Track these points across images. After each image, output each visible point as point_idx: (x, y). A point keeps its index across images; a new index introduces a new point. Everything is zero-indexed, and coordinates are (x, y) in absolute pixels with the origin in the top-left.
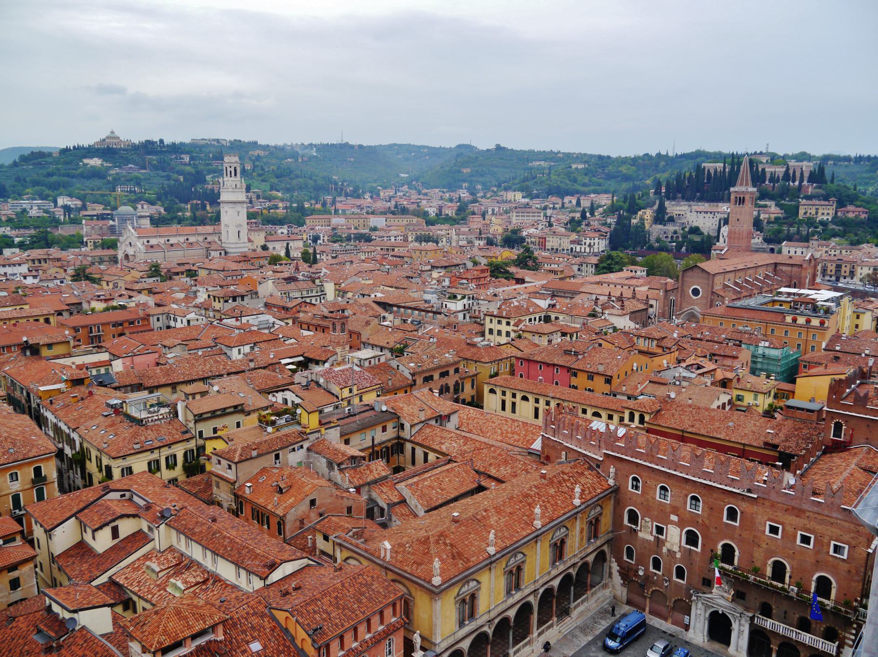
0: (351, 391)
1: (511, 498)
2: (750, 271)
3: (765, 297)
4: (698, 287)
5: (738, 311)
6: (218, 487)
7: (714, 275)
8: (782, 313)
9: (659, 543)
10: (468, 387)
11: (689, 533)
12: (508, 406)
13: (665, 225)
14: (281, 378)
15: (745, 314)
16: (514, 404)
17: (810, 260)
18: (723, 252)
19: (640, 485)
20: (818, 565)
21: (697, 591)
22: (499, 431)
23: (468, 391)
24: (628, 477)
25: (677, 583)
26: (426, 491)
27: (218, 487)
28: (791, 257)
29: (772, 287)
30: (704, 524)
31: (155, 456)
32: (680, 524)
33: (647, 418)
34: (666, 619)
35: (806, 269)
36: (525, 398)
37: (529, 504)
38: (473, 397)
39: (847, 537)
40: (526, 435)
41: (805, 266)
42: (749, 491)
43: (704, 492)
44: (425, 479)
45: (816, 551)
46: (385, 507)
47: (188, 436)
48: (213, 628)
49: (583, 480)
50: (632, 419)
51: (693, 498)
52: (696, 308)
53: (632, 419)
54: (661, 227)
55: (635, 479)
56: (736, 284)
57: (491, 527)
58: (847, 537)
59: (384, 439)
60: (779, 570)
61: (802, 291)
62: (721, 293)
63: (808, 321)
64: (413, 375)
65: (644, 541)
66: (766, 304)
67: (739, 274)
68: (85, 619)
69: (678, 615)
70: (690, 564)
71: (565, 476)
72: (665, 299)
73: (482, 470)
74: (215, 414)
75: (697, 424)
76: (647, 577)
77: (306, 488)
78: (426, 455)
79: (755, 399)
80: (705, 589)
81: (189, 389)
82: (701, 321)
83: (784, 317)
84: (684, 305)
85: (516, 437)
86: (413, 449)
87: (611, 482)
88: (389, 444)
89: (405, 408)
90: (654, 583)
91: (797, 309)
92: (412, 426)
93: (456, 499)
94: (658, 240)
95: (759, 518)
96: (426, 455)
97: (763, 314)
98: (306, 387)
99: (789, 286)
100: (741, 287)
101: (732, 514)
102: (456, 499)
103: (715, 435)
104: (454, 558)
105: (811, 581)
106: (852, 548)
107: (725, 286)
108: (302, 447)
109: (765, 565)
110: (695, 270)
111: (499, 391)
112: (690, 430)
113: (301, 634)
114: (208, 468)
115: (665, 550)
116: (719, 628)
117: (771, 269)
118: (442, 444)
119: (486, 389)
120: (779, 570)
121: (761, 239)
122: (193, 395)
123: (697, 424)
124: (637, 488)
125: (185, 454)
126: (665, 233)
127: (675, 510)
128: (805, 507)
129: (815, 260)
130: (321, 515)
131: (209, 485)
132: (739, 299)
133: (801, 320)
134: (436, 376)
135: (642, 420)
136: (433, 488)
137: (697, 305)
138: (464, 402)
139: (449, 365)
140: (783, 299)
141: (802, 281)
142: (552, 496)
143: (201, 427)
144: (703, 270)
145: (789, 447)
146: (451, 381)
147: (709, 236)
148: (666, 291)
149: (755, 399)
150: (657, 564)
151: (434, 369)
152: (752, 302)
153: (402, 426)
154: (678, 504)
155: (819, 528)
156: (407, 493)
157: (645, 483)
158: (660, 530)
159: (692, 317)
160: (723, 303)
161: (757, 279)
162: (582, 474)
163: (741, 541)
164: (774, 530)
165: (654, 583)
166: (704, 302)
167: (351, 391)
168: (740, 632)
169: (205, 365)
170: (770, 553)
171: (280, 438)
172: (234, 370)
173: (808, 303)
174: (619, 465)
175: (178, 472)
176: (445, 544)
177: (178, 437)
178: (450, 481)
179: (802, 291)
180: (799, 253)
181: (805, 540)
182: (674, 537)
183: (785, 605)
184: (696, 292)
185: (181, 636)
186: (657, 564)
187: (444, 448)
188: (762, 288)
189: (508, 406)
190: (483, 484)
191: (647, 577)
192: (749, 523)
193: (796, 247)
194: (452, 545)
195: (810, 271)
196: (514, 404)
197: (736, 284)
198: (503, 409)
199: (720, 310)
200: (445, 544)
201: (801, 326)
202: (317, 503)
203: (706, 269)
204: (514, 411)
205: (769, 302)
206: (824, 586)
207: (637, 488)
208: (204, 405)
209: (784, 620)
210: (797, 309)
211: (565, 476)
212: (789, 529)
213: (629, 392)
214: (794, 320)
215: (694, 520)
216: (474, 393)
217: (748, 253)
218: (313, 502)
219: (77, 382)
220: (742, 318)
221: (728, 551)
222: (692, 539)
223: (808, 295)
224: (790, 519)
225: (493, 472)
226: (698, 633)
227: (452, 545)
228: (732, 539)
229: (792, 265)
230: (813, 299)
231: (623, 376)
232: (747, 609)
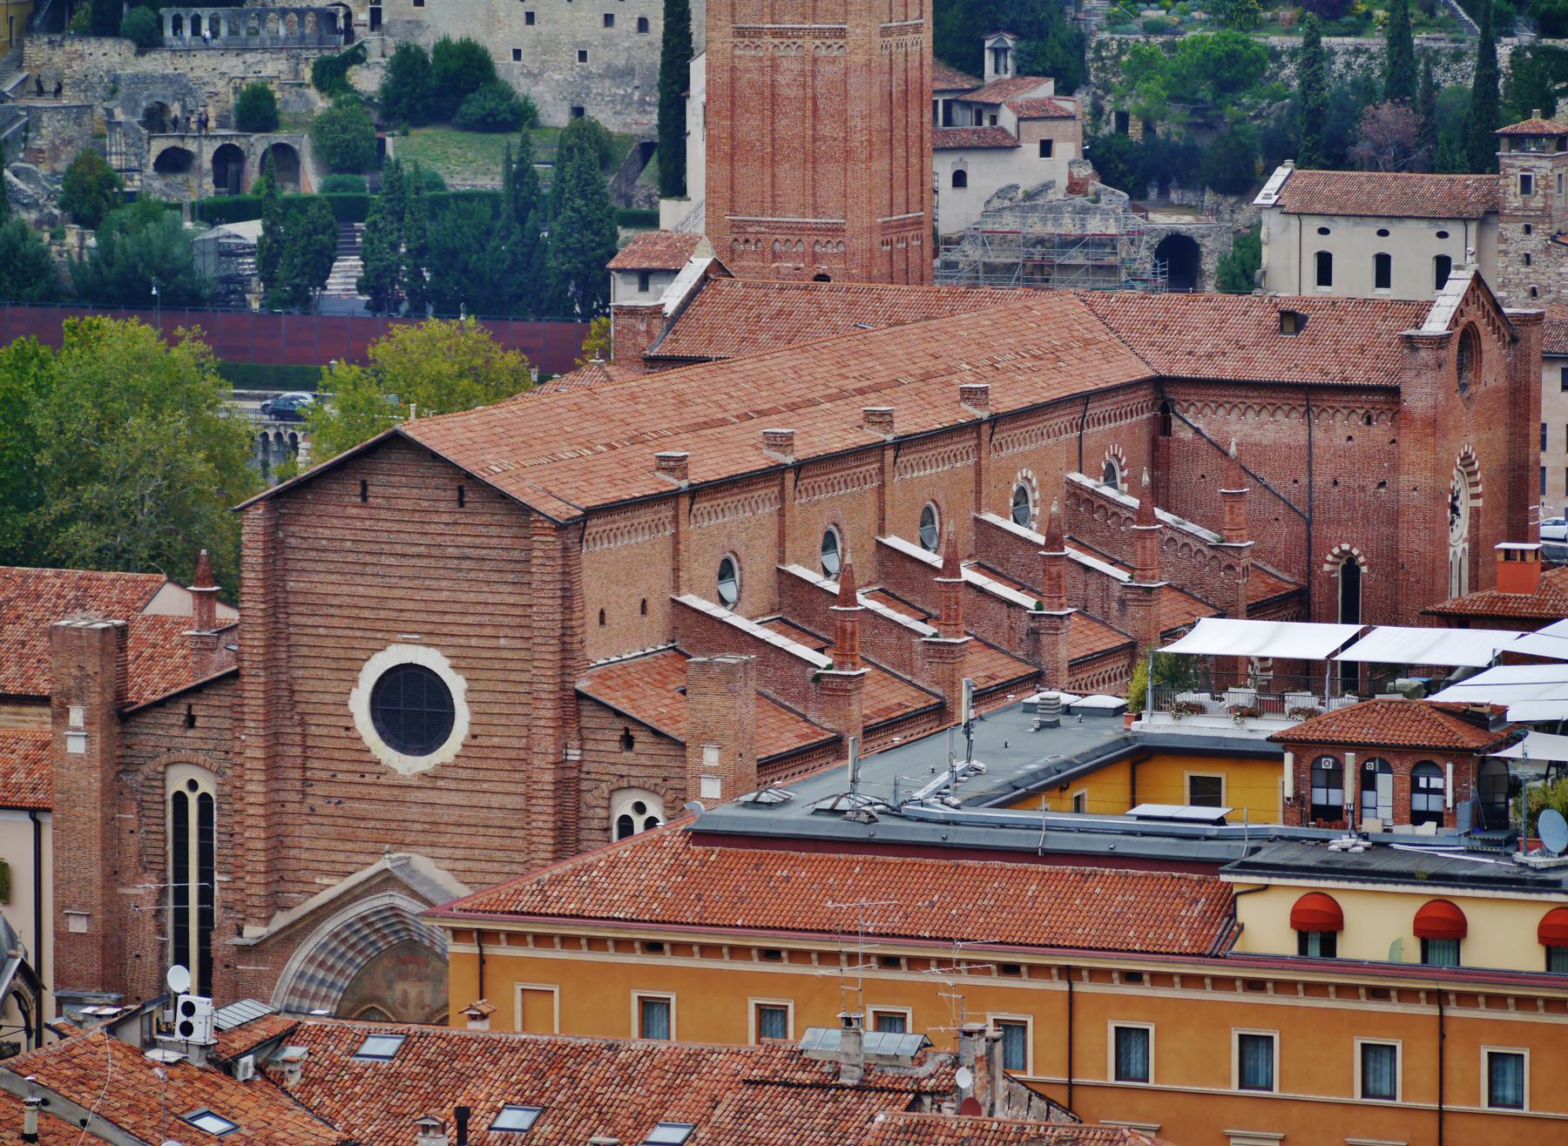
2: (926, 476)
3: (1053, 719)
4: (433, 659)
5: (799, 869)
7: (576, 527)
8: (1204, 872)
13: (148, 41)
15: (864, 899)
17: (1466, 339)
18: (671, 296)
28: (1292, 320)
29: (1135, 622)
35: (1434, 425)
41: (1420, 396)
52: (433, 872)
54: (108, 56)
56: (795, 603)
61: (1387, 644)
62: (651, 706)
63: (1442, 931)
66: (1061, 782)
67: (817, 507)
72: (114, 793)
82: (460, 990)
83: (1227, 905)
84: (308, 843)
91: (1331, 816)
94: (90, 195)
97: (1034, 882)
99: (1296, 605)
100: (836, 640)
107: (694, 634)
110: (395, 487)
117: (1120, 434)
121: (1067, 150)
126: (156, 119)
129: (1514, 331)
132: (834, 747)
133: (1378, 927)
137: (432, 834)
140: (1214, 724)
141: (1413, 541)
144: (467, 486)
147: (587, 144)
148: (124, 716)
152: (920, 779)
159: (388, 960)
160: (676, 804)
161: (993, 549)
166: (502, 797)
173: (1425, 759)
179: (1387, 644)
180: (1354, 278)
184: (412, 707)
188: (1039, 630)
193: (1385, 219)
195: (1475, 440)
197: (795, 603)
199: (625, 875)
201: (1379, 984)
203: (494, 467)
205: (1094, 768)
210: (1331, 816)
214: (1319, 928)
217: (905, 296)
220: (824, 944)
223: (1441, 676)
229: (1309, 396)
230: (1473, 716)
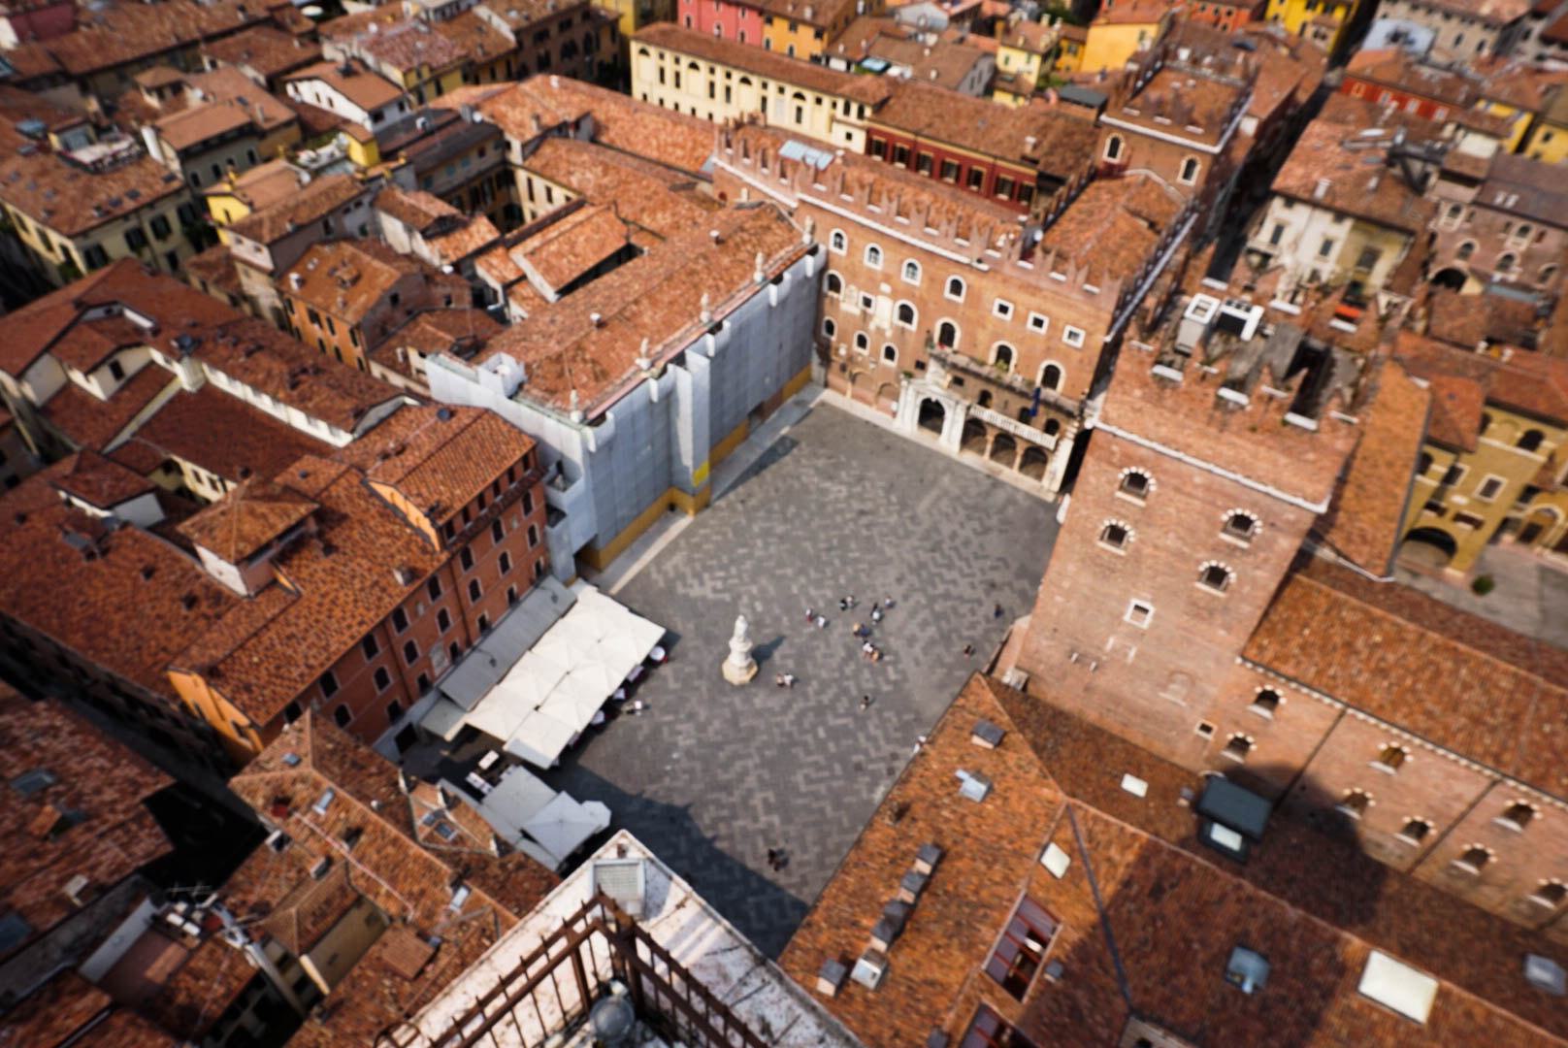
0: (419, 75)
1: (669, 278)
6: (248, 275)
9: (865, 317)
11: (904, 308)
16: (678, 75)
19: (845, 243)
20: (1048, 352)
21: (909, 375)
22: (654, 143)
24: (828, 231)
25: (886, 369)
26: (554, 261)
27: (248, 275)
30: (921, 298)
31: (132, 223)
32: (894, 295)
33: (868, 112)
34: (869, 403)
37: (695, 286)
38: (615, 57)
39: (1084, 323)
40: (694, 149)
42: (980, 261)
43: (924, 257)
44: (550, 241)
45: (1049, 338)
46: (498, 287)
47: (175, 185)
48: (301, 522)
49: (769, 238)
50: (847, 111)
51: (911, 265)
53: (847, 111)
55: (838, 235)
57: (644, 326)
58: (1084, 323)
59: (483, 167)
60: (1004, 354)
64: (517, 33)
65: (848, 315)
68: (125, 511)
69: (884, 401)
70: (902, 343)
71: (746, 236)
73: (631, 218)
74: (207, 146)
75: (937, 122)
76: (851, 358)
77: (382, 279)
78: (549, 191)
79: (1029, 62)
80: (917, 372)
85: (679, 152)
86: (530, 181)
87: (806, 238)
88: (493, 174)
89: (510, 114)
90: (858, 364)
92: (524, 146)
93: (596, 272)
95: (987, 295)
96: (549, 191)
98: (348, 72)
101: (956, 287)
102: (596, 272)
103: (958, 140)
104: (597, 379)
105: (1036, 369)
106: (1089, 334)
108: (359, 204)
109: (988, 349)
112: (926, 132)
113: (416, 515)
115: (872, 326)
116: (931, 414)
118: (570, 173)
119: (635, 47)
120: (1004, 354)
123: (937, 122)
124: (840, 246)
125: (180, 212)
127: (887, 278)
128: (1044, 284)
130: (409, 313)
134: (554, 30)
135: (861, 114)
136: (563, 256)
139: (571, 9)
142: (727, 270)
145: (1052, 164)
149: (1029, 62)
150: (862, 342)
151: (549, 20)
153: (508, 146)
154: (891, 271)
155: (1056, 310)
156: (526, 266)
157: (851, 241)
158: (867, 302)
162: (769, 228)
163: (965, 321)
164: (1003, 309)
165: (858, 364)
167: (419, 75)
168: (953, 422)
169: (162, 22)
170: (996, 336)
171: (326, 193)
172: (214, 29)
174: (818, 215)
176: (585, 361)
177: (160, 188)
178: (587, 240)
181: (1038, 323)
182: (885, 312)
183: (1007, 395)
185: (264, 540)
186: (862, 342)
187: (574, 180)
190: (633, 240)
191: (851, 358)
192: (975, 300)
194: (594, 362)
196: (678, 75)
198: (662, 80)
200: (585, 361)
202: (401, 298)
204: (678, 85)
206: (1051, 376)
207: (840, 246)
209: (1004, 410)
211: (746, 236)
212: (1020, 308)
213: (849, 54)
215: (909, 292)
216: (615, 49)
218: (395, 299)
221: (947, 334)
222: (906, 314)
224: (1023, 298)
225: (646, 221)
226: (905, 422)
227: (594, 362)
228: (954, 316)
231: (841, 24)
232: (965, 397)
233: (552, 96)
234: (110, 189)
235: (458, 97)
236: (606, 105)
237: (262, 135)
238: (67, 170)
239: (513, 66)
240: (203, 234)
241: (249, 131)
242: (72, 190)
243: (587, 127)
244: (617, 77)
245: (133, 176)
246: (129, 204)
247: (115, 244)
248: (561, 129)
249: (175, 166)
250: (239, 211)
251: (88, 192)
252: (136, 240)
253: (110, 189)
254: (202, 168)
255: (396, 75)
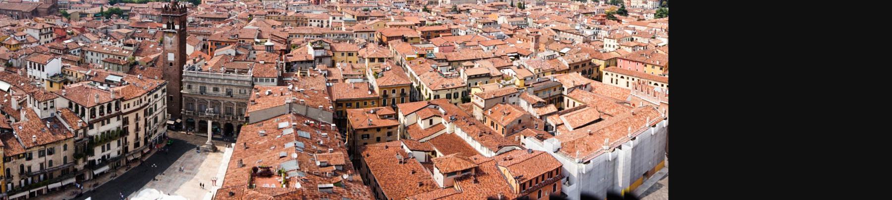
10: (595, 72)
12: (614, 81)
14: (506, 63)
23: (595, 74)
36: (622, 77)
74: (476, 76)
81: (465, 64)
111: (610, 73)
114: (472, 100)
122: (467, 67)
131: (472, 108)
138: (593, 79)
143: (470, 81)
146: (587, 68)
175: (459, 99)
189: (614, 81)
208: (472, 72)
219: (422, 56)
233: (577, 78)
234: (447, 82)
235: (549, 76)
236: (594, 84)
237: (492, 77)
238: (439, 76)
239: (567, 71)
240: (466, 99)
241: (488, 75)
242: (438, 80)
243: (588, 87)
244: (599, 79)
245: (454, 81)
246: (451, 87)
247: (443, 95)
248: (581, 87)
249: (466, 80)
250: (478, 91)
251: (442, 81)
252: (449, 96)
253: (447, 82)
254: (472, 82)
255: (532, 70)
